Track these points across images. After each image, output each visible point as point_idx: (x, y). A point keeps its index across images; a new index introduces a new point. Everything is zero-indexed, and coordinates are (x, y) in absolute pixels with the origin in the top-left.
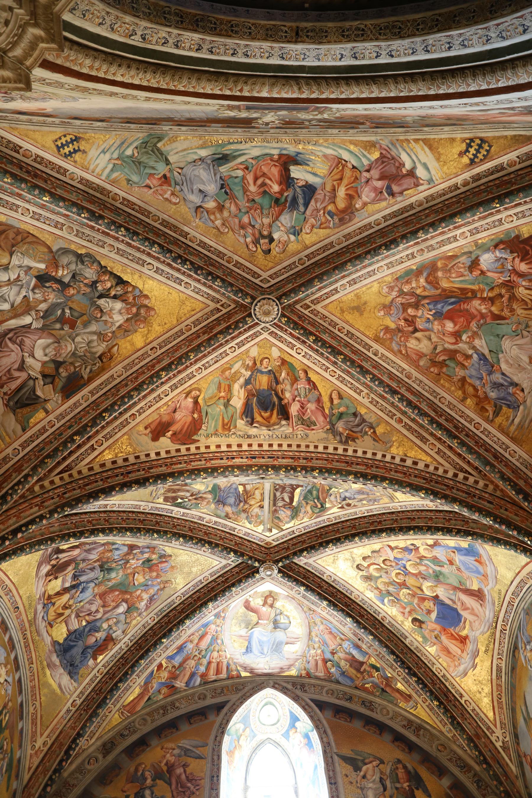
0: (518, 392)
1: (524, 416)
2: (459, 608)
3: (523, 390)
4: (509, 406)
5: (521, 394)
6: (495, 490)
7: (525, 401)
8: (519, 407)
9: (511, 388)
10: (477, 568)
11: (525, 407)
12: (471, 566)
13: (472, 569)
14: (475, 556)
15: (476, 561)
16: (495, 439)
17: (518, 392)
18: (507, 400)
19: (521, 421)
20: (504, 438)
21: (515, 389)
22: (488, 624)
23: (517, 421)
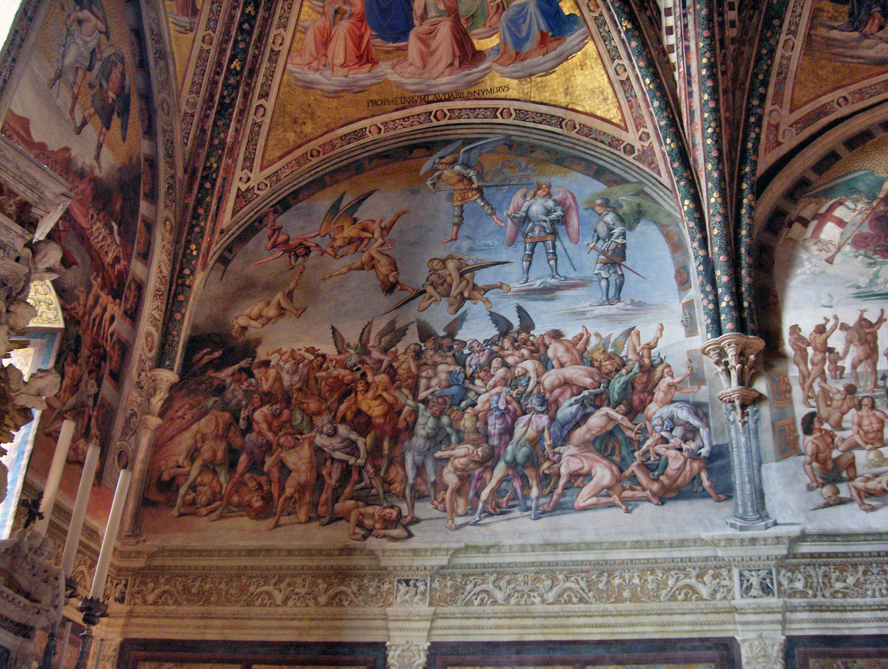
0: (876, 21)
1: (845, 42)
2: (419, 28)
3: (881, 28)
4: (851, 14)
5: (875, 28)
6: (733, 41)
7: (866, 37)
8: (856, 30)
9: (879, 8)
10: (527, 37)
11: (858, 40)
12: (524, 28)
13: (519, 31)
14: (551, 29)
15: (543, 35)
16: (799, 10)
17: (876, 21)
18: (859, 9)
19: (839, 41)
20: (805, 23)
21: (878, 15)
22: (423, 87)
23: (835, 34)
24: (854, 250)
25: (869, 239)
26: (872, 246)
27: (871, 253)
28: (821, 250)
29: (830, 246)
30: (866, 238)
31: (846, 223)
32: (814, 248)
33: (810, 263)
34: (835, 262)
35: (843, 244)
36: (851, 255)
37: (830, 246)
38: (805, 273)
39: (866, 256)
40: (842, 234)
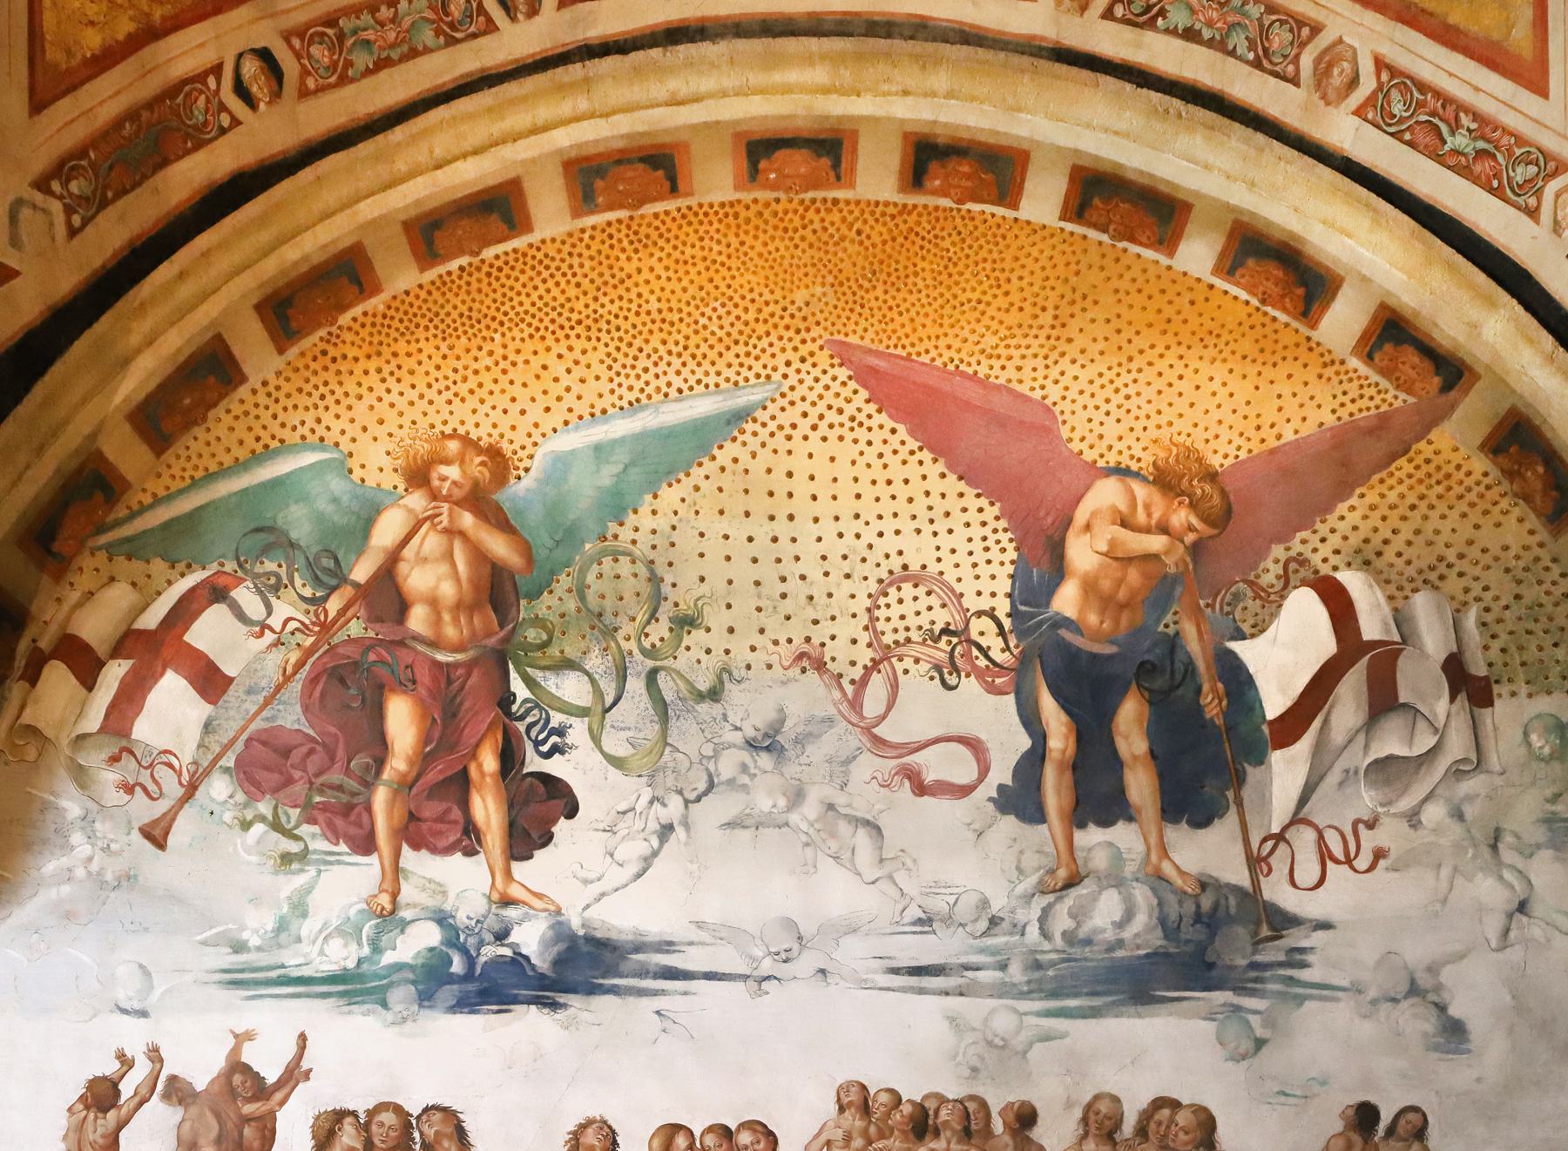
24: (240, 797)
25: (296, 756)
26: (300, 788)
27: (295, 813)
28: (129, 789)
29: (162, 773)
30: (286, 753)
31: (230, 680)
32: (110, 776)
33: (91, 837)
34: (171, 840)
35: (207, 772)
36: (228, 817)
37: (162, 773)
38: (68, 876)
39: (276, 826)
40: (208, 727)
